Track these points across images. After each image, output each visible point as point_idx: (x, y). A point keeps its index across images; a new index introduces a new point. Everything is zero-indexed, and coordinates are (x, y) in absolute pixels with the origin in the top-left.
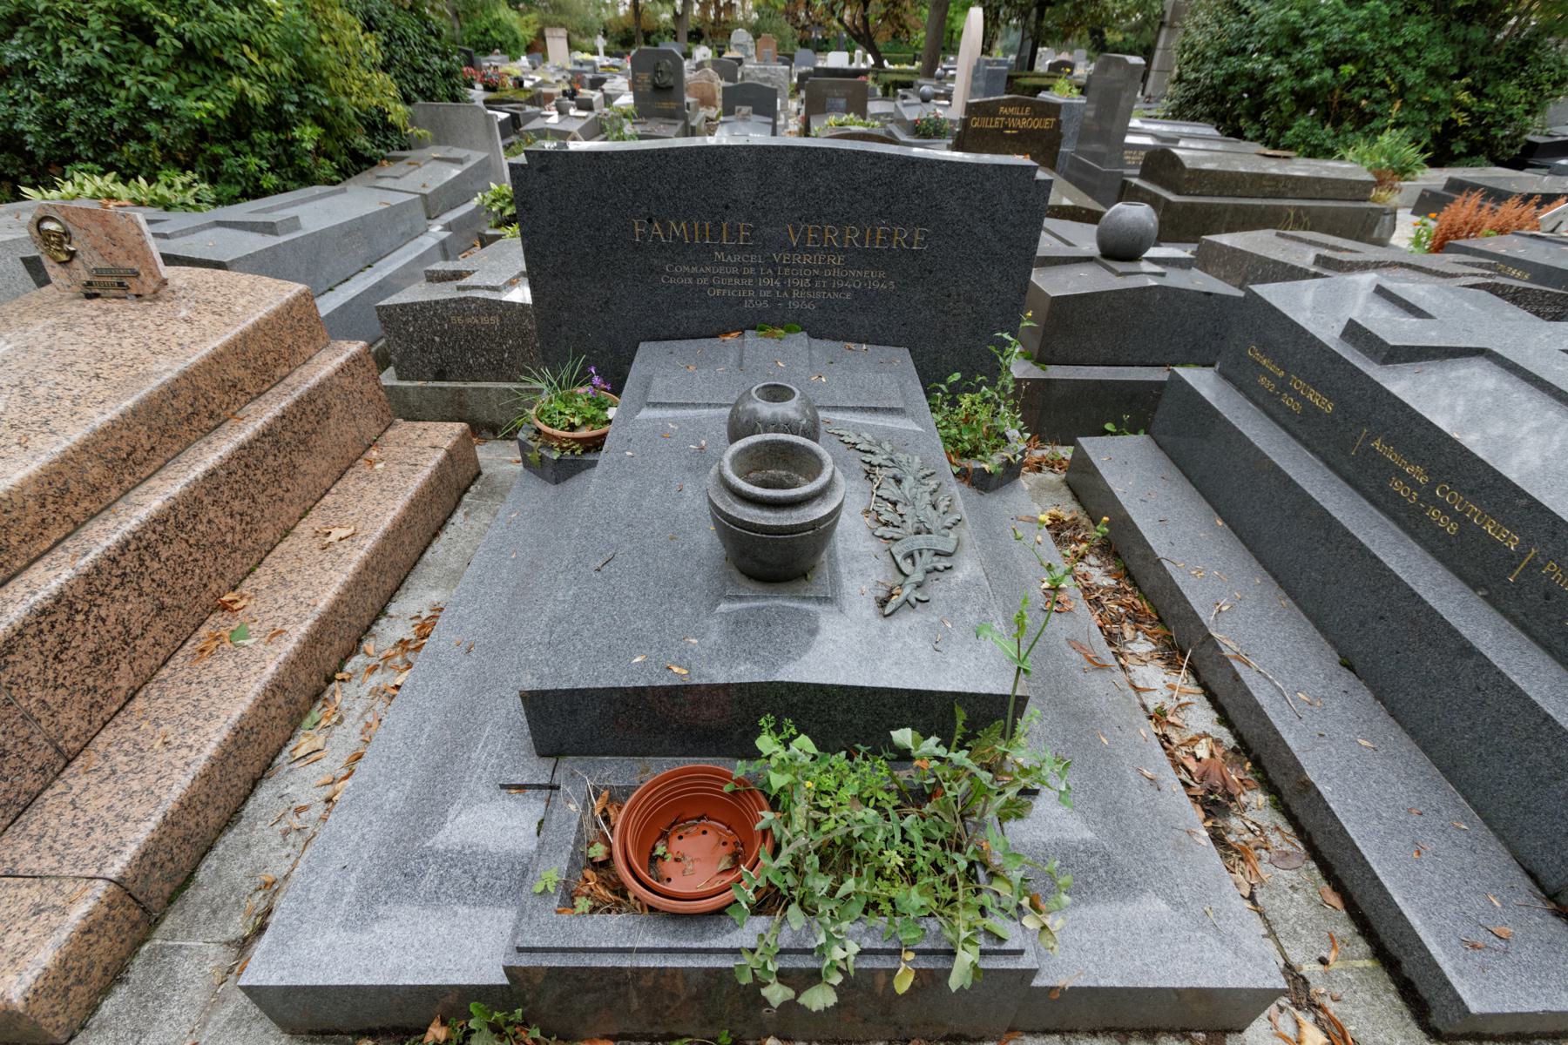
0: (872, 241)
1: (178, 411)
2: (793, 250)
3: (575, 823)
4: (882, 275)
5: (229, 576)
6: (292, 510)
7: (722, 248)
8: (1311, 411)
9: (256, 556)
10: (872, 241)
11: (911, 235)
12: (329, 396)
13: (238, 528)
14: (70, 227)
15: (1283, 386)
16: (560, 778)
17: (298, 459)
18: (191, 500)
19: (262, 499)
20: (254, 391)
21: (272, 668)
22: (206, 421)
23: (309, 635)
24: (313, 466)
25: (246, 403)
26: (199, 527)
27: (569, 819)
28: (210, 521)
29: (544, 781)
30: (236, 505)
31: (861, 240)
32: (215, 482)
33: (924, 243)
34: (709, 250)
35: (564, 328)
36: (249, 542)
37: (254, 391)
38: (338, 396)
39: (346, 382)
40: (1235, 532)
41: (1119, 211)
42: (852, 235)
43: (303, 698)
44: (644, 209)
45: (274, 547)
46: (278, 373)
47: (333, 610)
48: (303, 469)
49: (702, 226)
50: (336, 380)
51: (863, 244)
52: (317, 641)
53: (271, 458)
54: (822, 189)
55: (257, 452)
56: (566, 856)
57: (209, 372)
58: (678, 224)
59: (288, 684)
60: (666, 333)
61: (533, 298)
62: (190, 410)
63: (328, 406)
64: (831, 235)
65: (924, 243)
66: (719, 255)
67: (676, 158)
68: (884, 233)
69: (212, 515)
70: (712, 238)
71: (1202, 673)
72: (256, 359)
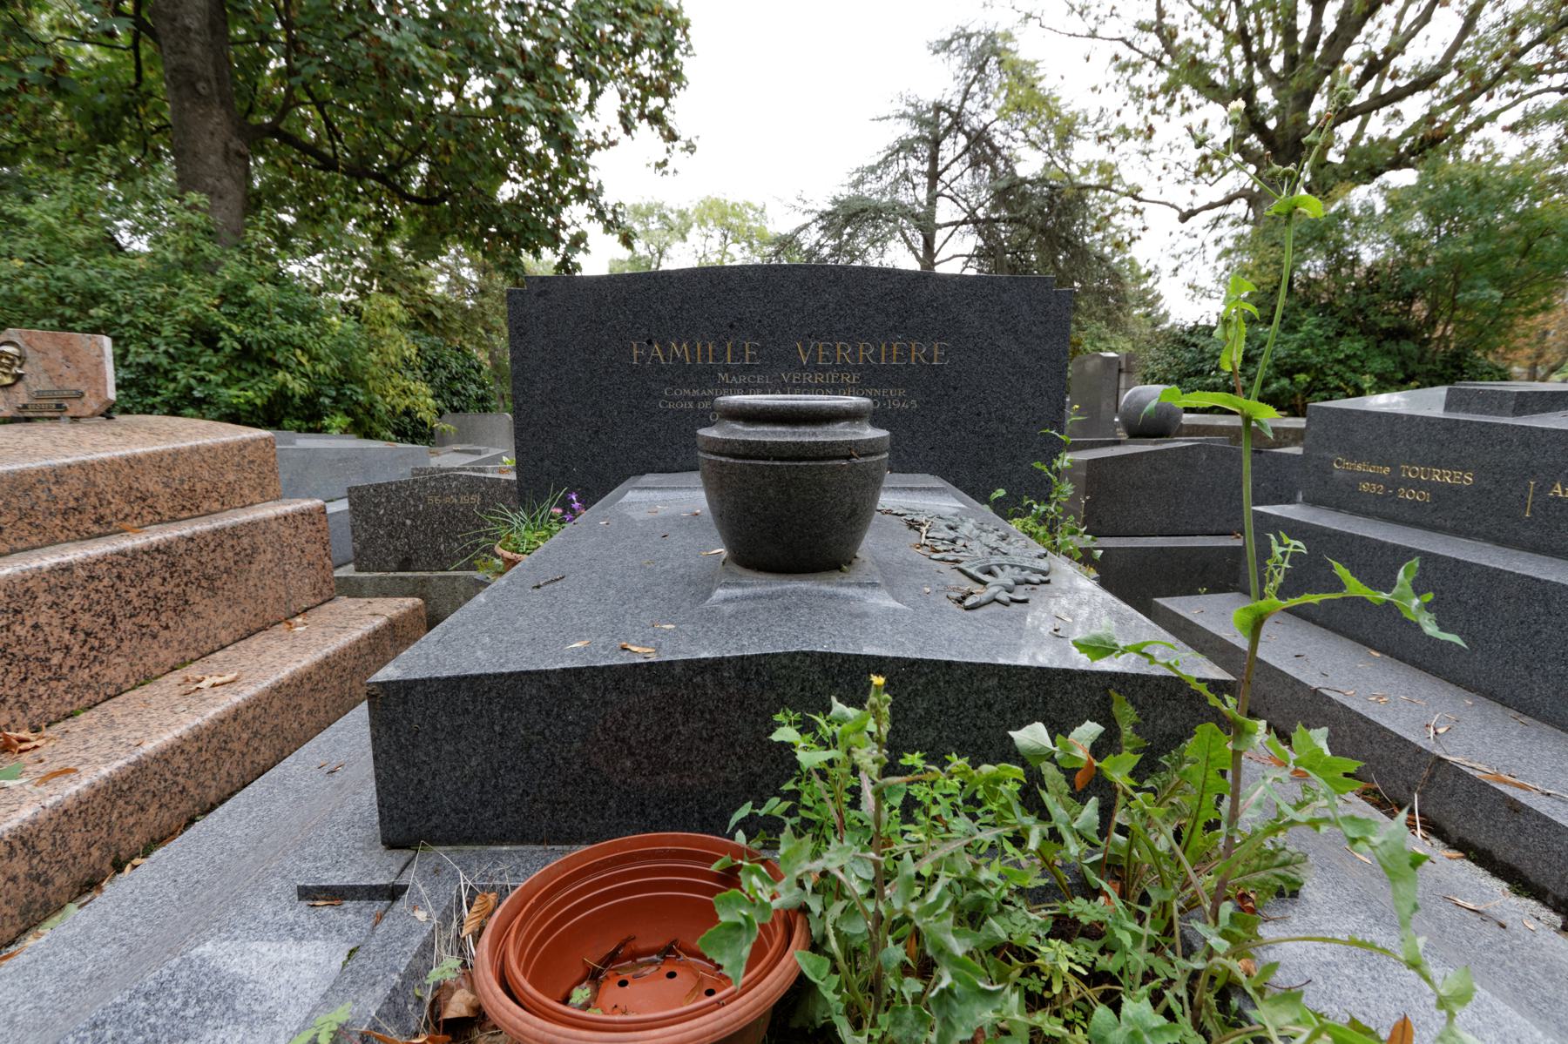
0: (889, 357)
1: (55, 500)
2: (803, 369)
3: (417, 941)
4: (902, 392)
5: (36, 709)
6: (163, 654)
7: (727, 369)
8: (1442, 494)
9: (89, 696)
10: (889, 357)
11: (930, 350)
12: (259, 539)
13: (76, 649)
14: (28, 351)
15: (1394, 483)
16: (411, 878)
17: (195, 596)
18: (19, 589)
19: (126, 625)
20: (167, 515)
21: (27, 813)
22: (88, 524)
23: (111, 781)
24: (214, 615)
25: (152, 523)
26: (17, 628)
27: (409, 933)
28: (36, 626)
29: (381, 880)
30: (85, 620)
31: (877, 356)
32: (65, 579)
33: (945, 357)
34: (712, 373)
35: (547, 462)
36: (85, 674)
37: (167, 515)
38: (271, 544)
39: (286, 532)
40: (1401, 659)
41: (1135, 394)
42: (865, 352)
43: (61, 879)
44: (644, 331)
45: (120, 692)
46: (206, 505)
47: (164, 757)
48: (197, 609)
49: (705, 347)
50: (274, 525)
51: (878, 360)
52: (121, 794)
53: (157, 580)
54: (832, 306)
55: (141, 567)
56: (381, 992)
57: (117, 473)
58: (679, 345)
59: (44, 845)
60: (662, 465)
61: (519, 467)
62: (72, 504)
63: (255, 549)
64: (842, 352)
65: (945, 357)
66: (723, 377)
67: (680, 279)
68: (900, 348)
69: (43, 619)
70: (715, 358)
71: (1449, 827)
72: (182, 482)
